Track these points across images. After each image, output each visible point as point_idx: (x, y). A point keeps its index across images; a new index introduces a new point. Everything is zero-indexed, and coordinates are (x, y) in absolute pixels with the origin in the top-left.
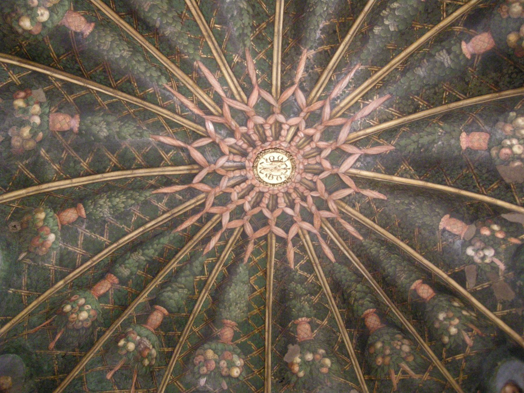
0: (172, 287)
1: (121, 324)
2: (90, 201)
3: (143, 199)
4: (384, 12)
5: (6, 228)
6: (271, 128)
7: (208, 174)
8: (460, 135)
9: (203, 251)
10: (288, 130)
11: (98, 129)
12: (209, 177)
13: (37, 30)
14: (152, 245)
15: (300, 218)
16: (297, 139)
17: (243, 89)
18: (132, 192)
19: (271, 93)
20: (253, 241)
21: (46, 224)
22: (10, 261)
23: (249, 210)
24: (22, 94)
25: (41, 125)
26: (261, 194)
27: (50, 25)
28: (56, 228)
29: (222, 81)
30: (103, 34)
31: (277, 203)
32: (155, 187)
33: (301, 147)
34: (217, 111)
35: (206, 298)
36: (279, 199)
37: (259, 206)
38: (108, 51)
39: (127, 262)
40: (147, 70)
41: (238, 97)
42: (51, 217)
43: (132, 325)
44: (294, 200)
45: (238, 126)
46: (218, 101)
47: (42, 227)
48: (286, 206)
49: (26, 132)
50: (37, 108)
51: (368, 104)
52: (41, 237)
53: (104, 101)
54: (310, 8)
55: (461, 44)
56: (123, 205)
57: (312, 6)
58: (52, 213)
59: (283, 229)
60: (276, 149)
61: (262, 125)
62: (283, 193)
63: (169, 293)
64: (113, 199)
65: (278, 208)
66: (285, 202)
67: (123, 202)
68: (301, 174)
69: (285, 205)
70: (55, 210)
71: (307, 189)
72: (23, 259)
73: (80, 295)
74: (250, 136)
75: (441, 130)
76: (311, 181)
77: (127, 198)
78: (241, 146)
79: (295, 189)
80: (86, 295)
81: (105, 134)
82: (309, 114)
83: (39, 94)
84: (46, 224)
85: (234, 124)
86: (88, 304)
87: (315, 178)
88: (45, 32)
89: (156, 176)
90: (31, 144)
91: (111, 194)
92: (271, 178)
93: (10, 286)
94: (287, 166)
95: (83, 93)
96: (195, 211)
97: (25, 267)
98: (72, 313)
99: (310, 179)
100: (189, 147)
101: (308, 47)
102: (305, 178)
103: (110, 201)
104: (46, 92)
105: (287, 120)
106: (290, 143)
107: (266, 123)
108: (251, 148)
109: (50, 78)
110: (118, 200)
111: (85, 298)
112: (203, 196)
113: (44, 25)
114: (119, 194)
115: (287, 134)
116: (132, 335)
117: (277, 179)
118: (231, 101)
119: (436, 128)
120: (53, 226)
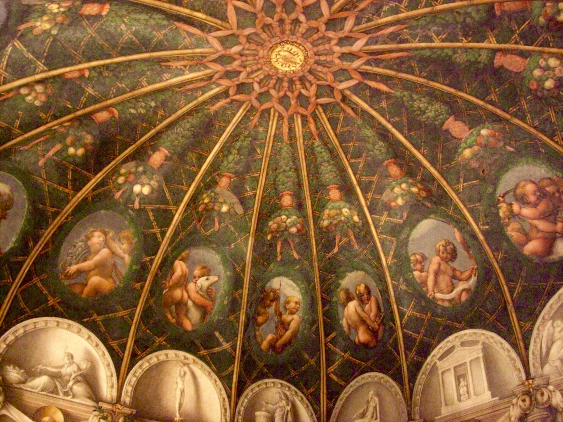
0: (465, 19)
1: (532, 45)
2: (437, 123)
3: (405, 93)
4: (142, 112)
5: (487, 177)
6: (269, 84)
7: (341, 82)
8: (108, 13)
9: (405, 28)
10: (257, 76)
11: (382, 148)
12: (343, 79)
13: (356, 213)
14: (439, 55)
15: (297, 8)
16: (255, 68)
17: (269, 114)
18: (406, 104)
19: (252, 106)
20: (356, 10)
21: (474, 143)
22: (517, 158)
23: (334, 39)
24: (393, 204)
25: (404, 182)
26: (314, 44)
27: (348, 206)
28: (474, 133)
29: (279, 127)
30: (328, 180)
31: (307, 30)
32: (388, 96)
33: (256, 62)
34: (297, 117)
35: (443, 3)
36: (303, 32)
37: (324, 36)
38: (335, 172)
39: (473, 59)
40: (321, 153)
41: (277, 114)
42: (465, 142)
43: (534, 23)
44: (291, 24)
45: (291, 99)
46: (291, 119)
47: (477, 145)
48: (301, 22)
49: (415, 190)
50: (397, 190)
51: (182, 66)
52: (487, 141)
53: (360, 162)
54: (193, 131)
55: (89, 76)
56: (423, 99)
57: (191, 131)
58: (463, 145)
59: (319, 7)
60: (277, 69)
61: (274, 88)
62: (296, 35)
63: (474, 14)
64: (423, 109)
65: (309, 27)
66: (300, 27)
67: (421, 101)
68: (269, 40)
69: (301, 25)
70: (456, 148)
71: (273, 28)
72: (513, 147)
73: (529, 81)
74: (289, 87)
75: (125, 20)
76: (265, 32)
77: (415, 101)
78: (301, 84)
79: (283, 33)
80: (529, 72)
81: (382, 143)
82: (233, 80)
83: (385, 197)
84: (474, 143)
85: (293, 102)
86: (539, 64)
87: (260, 31)
88: (353, 207)
89: (375, 110)
90: (419, 185)
91: (420, 115)
92: (296, 53)
93: (539, 152)
94: (276, 55)
95: (364, 179)
96: (377, 63)
97: (518, 143)
98: (554, 75)
99: (265, 34)
100: (339, 101)
101: (208, 111)
102: (268, 36)
103: (427, 109)
104: (381, 194)
105: (253, 83)
106: (262, 69)
107: (269, 88)
108: (294, 79)
109: (368, 204)
110: (421, 105)
111: (532, 71)
112: (359, 70)
113: (350, 209)
114: (415, 109)
115: (260, 75)
116: (548, 11)
117: (292, 49)
118: (283, 114)
119: (129, 23)
120: (474, 135)
